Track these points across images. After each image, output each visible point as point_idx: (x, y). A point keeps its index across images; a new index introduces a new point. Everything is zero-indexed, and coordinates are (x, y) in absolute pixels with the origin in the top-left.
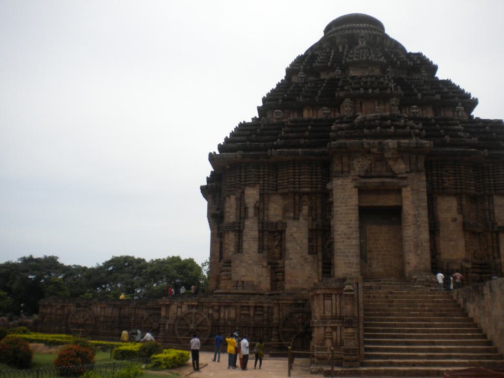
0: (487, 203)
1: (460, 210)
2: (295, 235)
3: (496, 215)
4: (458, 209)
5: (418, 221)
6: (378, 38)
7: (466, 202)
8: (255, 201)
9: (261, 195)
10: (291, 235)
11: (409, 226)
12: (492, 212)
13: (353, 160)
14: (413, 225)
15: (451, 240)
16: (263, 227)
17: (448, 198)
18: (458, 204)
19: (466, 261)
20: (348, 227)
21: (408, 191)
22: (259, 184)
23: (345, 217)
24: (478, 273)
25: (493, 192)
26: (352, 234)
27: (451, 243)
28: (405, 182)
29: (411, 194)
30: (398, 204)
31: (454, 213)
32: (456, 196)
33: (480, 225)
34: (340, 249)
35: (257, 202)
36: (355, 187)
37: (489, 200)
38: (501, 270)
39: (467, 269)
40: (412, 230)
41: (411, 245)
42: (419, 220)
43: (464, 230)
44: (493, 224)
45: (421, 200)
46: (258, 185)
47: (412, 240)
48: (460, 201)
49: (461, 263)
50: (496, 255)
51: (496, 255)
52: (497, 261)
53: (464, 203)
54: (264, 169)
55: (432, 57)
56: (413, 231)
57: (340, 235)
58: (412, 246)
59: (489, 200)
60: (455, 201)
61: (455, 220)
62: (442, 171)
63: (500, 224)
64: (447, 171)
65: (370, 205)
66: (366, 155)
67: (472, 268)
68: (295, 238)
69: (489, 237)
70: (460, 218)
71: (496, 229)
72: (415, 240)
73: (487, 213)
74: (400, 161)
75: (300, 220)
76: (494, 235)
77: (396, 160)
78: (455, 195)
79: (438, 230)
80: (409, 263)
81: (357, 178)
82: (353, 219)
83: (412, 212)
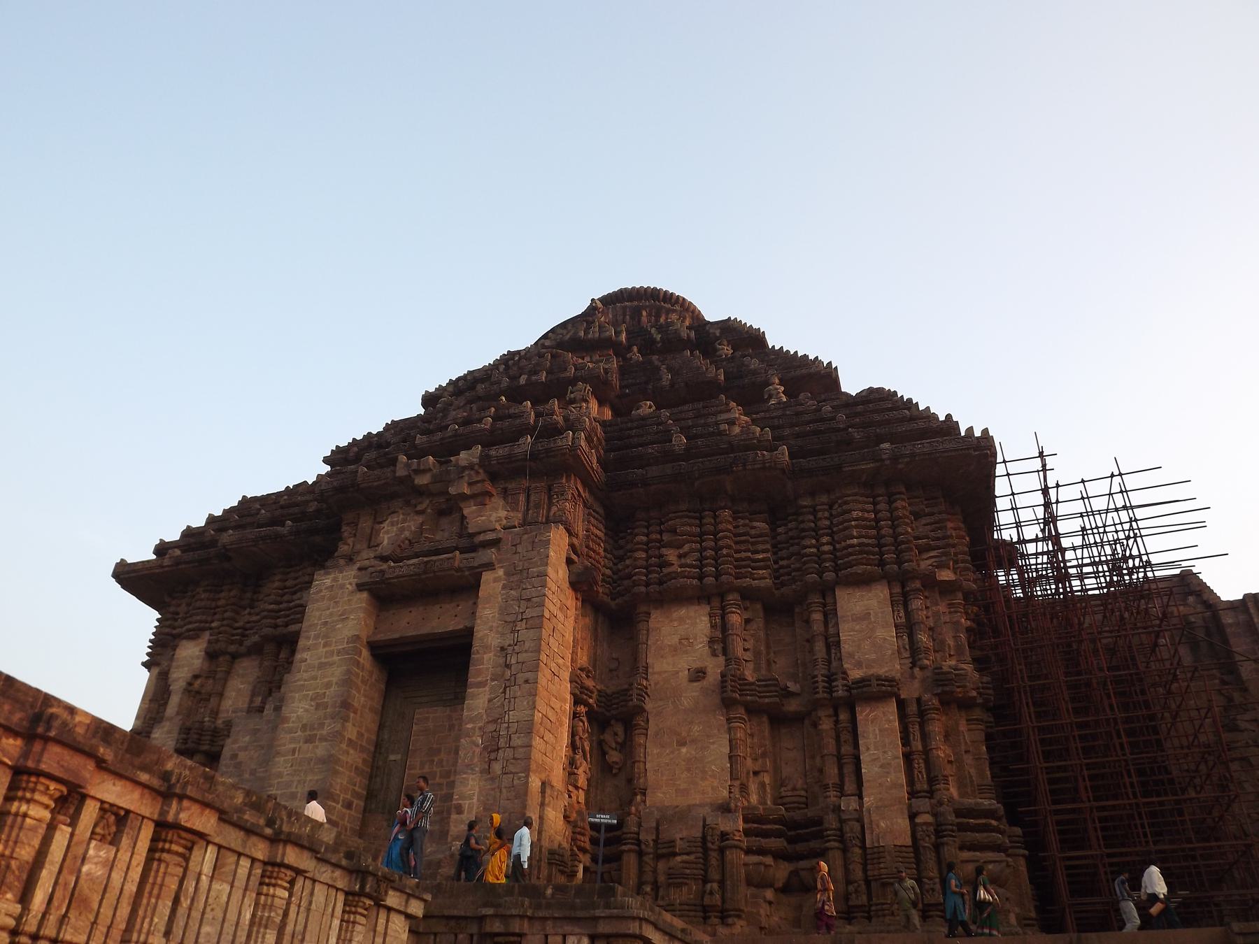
0: (817, 616)
1: (721, 641)
2: (242, 756)
3: (846, 648)
4: (712, 641)
5: (508, 666)
6: (644, 313)
7: (747, 621)
8: (190, 675)
9: (211, 655)
10: (234, 756)
11: (482, 684)
12: (833, 644)
13: (381, 523)
14: (492, 680)
15: (682, 743)
16: (185, 741)
17: (683, 612)
18: (713, 626)
19: (725, 809)
20: (318, 706)
21: (496, 580)
22: (211, 629)
23: (315, 678)
24: (779, 856)
25: (829, 576)
26: (322, 725)
27: (684, 750)
28: (491, 554)
29: (504, 587)
30: (468, 624)
31: (699, 654)
32: (709, 604)
33: (792, 687)
34: (280, 775)
35: (196, 677)
36: (360, 587)
37: (825, 605)
38: (863, 841)
39: (724, 836)
40: (487, 697)
41: (478, 746)
42: (513, 661)
43: (727, 704)
44: (830, 679)
45: (529, 600)
46: (207, 633)
47: (480, 728)
48: (723, 618)
49: (704, 820)
50: (850, 787)
51: (850, 787)
52: (849, 804)
53: (735, 619)
54: (230, 590)
55: (751, 319)
56: (490, 701)
57: (291, 731)
58: (478, 750)
59: (825, 605)
60: (706, 619)
61: (698, 675)
62: (661, 533)
63: (856, 674)
64: (674, 531)
65: (396, 636)
66: (413, 502)
67: (747, 833)
68: (240, 763)
69: (826, 725)
70: (715, 667)
71: (841, 693)
72: (491, 727)
73: (820, 647)
74: (498, 501)
75: (266, 712)
76: (843, 716)
77: (481, 498)
78: (701, 597)
79: (641, 710)
80: (459, 810)
81: (377, 562)
82: (334, 680)
83: (494, 640)
